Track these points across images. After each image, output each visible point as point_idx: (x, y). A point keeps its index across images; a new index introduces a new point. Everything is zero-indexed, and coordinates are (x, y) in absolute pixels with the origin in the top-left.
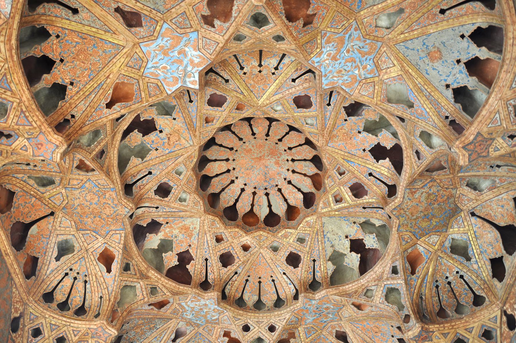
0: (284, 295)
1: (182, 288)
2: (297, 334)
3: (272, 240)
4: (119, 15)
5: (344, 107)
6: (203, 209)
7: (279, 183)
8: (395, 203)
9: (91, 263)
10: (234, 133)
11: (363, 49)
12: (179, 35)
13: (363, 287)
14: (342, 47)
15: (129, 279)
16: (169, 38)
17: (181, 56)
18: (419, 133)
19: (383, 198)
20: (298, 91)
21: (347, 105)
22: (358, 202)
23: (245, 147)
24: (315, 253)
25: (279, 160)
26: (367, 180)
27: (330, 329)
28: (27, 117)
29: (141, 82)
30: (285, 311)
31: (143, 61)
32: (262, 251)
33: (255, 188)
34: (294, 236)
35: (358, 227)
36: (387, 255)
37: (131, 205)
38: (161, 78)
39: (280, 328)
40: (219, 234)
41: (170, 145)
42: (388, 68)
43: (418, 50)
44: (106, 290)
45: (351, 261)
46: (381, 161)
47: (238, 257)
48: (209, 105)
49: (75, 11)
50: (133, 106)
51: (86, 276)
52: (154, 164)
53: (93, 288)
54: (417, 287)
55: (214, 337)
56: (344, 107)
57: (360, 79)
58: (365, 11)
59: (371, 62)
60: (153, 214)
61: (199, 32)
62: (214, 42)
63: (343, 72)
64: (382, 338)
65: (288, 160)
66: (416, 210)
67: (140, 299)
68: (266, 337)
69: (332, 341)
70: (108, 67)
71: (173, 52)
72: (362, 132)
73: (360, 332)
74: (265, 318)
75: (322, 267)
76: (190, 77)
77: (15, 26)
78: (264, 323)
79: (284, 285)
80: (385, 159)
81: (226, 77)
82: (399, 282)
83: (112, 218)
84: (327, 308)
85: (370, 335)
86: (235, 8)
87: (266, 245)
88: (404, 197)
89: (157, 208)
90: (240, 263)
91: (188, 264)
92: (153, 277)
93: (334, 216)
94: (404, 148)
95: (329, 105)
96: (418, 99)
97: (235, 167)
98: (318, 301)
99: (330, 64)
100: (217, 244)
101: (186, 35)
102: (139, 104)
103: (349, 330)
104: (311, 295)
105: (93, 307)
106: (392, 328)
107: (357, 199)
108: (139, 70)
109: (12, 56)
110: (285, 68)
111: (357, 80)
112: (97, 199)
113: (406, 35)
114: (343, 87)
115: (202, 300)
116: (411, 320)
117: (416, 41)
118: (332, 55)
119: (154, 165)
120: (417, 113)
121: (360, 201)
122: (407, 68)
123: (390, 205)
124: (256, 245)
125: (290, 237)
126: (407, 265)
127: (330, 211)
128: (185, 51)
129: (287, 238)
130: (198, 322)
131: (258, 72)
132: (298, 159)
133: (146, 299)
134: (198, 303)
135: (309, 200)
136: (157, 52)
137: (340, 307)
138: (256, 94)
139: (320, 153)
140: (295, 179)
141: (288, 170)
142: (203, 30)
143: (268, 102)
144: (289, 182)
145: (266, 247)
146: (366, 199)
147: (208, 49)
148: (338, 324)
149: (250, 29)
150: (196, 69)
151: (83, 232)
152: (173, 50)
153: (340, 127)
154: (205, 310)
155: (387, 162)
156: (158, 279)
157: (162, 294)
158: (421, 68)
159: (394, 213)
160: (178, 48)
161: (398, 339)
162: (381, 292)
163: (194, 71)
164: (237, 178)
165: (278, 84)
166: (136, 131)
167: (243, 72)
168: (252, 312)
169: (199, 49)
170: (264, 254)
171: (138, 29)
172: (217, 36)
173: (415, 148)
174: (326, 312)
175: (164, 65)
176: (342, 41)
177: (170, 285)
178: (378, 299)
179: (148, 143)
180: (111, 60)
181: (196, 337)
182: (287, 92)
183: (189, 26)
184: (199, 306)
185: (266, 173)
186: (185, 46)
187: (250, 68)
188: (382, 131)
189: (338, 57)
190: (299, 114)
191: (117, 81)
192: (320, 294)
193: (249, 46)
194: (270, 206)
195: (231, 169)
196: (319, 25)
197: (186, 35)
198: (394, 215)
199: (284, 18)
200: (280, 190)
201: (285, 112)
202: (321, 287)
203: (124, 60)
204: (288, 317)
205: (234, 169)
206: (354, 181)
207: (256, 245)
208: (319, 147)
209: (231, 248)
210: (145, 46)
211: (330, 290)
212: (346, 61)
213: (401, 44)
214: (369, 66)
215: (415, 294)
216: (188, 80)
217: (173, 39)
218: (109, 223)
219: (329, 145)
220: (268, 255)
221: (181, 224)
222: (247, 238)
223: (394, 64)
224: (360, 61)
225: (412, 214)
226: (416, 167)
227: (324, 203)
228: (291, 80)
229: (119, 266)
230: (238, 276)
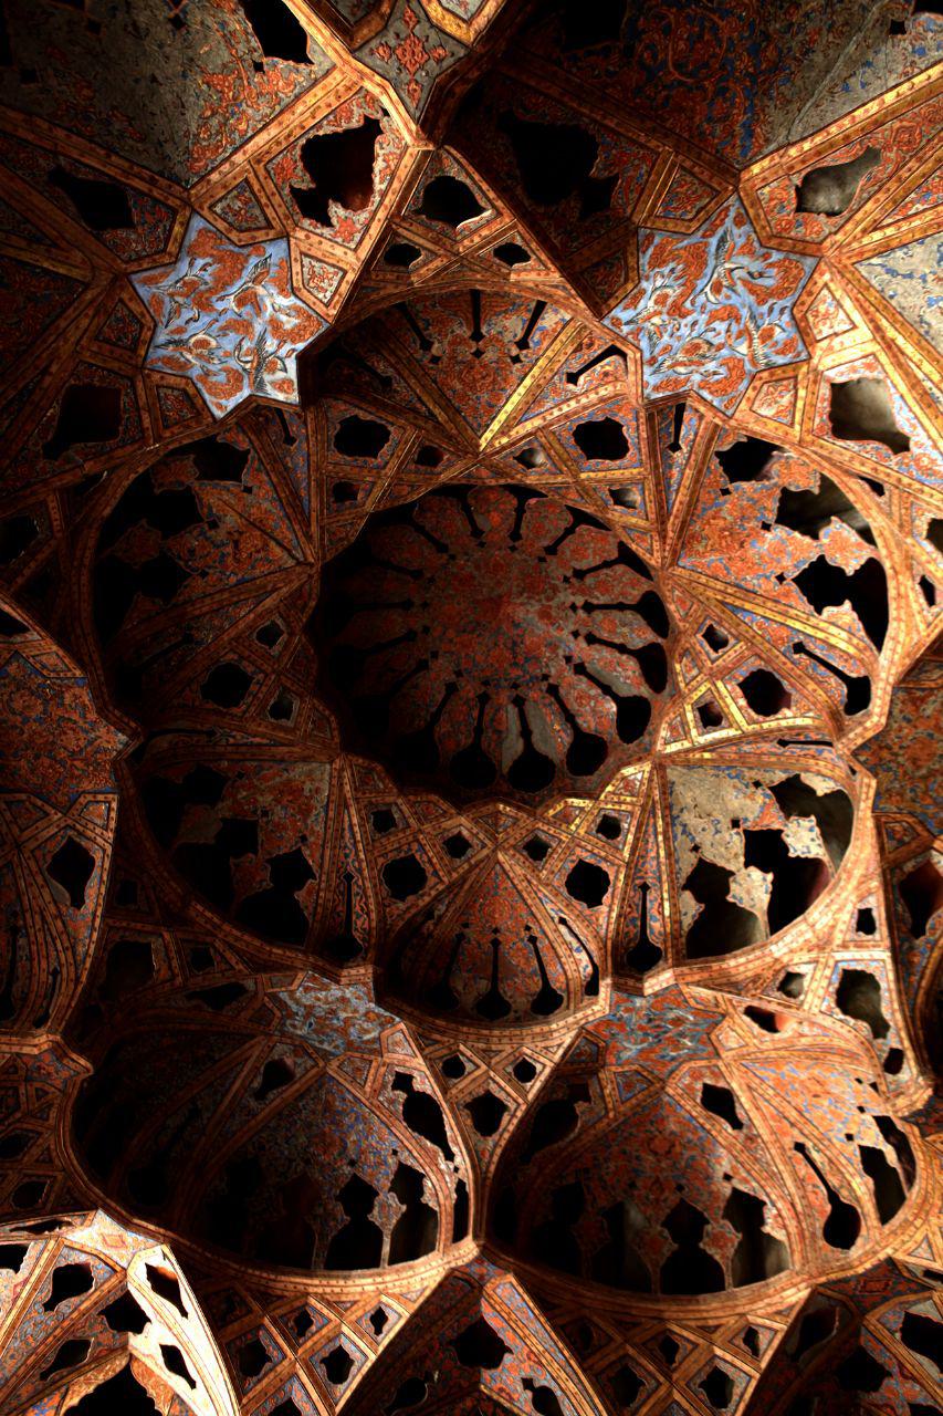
0: (562, 979)
1: (280, 952)
2: (593, 1090)
3: (529, 827)
6: (337, 740)
7: (553, 671)
8: (866, 729)
9: (31, 880)
10: (420, 529)
11: (759, 281)
12: (236, 249)
13: (778, 967)
14: (697, 278)
15: (133, 925)
16: (209, 260)
17: (247, 310)
18: (926, 527)
19: (834, 716)
20: (585, 408)
22: (765, 726)
23: (455, 570)
24: (648, 866)
25: (550, 607)
26: (789, 665)
27: (687, 1080)
29: (140, 386)
30: (562, 1023)
31: (142, 326)
32: (500, 856)
33: (486, 683)
34: (591, 818)
35: (766, 796)
36: (844, 876)
37: (133, 725)
38: (195, 373)
39: (547, 1071)
40: (384, 808)
41: (238, 561)
42: (836, 334)
43: (924, 279)
44: (70, 953)
45: (748, 892)
46: (828, 611)
47: (435, 873)
50: (120, 452)
51: (15, 914)
52: (197, 612)
53: (34, 948)
54: (928, 972)
55: (368, 1089)
56: (718, 454)
57: (754, 370)
58: (766, 163)
59: (786, 317)
60: (199, 750)
61: (293, 241)
62: (332, 270)
63: (705, 347)
64: (832, 1112)
65: (574, 607)
66: (927, 752)
67: (161, 977)
68: (509, 1095)
69: (694, 1114)
70: (44, 341)
71: (222, 299)
72: (774, 526)
73: (771, 1092)
74: (505, 1040)
75: (667, 905)
76: (273, 371)
78: (504, 1054)
79: (561, 954)
80: (839, 603)
81: (381, 367)
82: (875, 957)
83: (82, 760)
84: (678, 1021)
85: (799, 1101)
86: (379, 165)
87: (512, 841)
88: (890, 713)
89: (211, 734)
90: (441, 887)
91: (300, 889)
92: (202, 921)
93: (701, 763)
94: (889, 572)
95: (676, 447)
96: (922, 425)
97: (426, 622)
98: (652, 1001)
99: (664, 326)
100: (378, 835)
101: (257, 250)
102: (136, 446)
103: (740, 1085)
104: (631, 982)
105: (32, 997)
106: (860, 1087)
107: (761, 718)
108: (134, 351)
111: (743, 373)
112: (41, 708)
113: (890, 231)
114: (705, 394)
115: (334, 986)
116: (905, 1066)
117: (918, 250)
118: (670, 301)
119: (199, 617)
120: (919, 468)
121: (770, 723)
122: (891, 333)
123: (851, 735)
124: (487, 841)
125: (577, 821)
126: (900, 908)
127: (687, 751)
128: (256, 295)
129: (573, 822)
130: (326, 1046)
131: (470, 357)
132: (602, 602)
133: (179, 980)
134: (322, 995)
135: (635, 719)
136: (180, 299)
137: (713, 1018)
138: (470, 419)
139: (658, 583)
140: (598, 657)
141: (576, 634)
142: (301, 234)
143: (505, 440)
144: (580, 669)
145: (514, 847)
146: (787, 718)
148: (708, 1067)
149: (429, 229)
150: (288, 347)
151: (9, 797)
152: (223, 294)
153: (711, 513)
154: (343, 1015)
155: (845, 612)
156: (215, 926)
157: (224, 966)
158: (932, 332)
159: (862, 758)
160: (235, 289)
161: (875, 1117)
162: (825, 983)
163: (283, 352)
164: (435, 655)
165: (529, 390)
167: (428, 357)
168: (469, 1025)
169: (294, 291)
170: (507, 867)
171: (122, 233)
172: (339, 251)
173: (918, 571)
174: (673, 1030)
175: (201, 336)
176: (697, 259)
177: (248, 944)
178: (817, 1001)
179: (180, 558)
180: (53, 322)
181: (321, 1087)
182: (556, 413)
183: (263, 223)
184: (327, 1002)
185: (515, 643)
186: (254, 281)
187: (452, 343)
188: (829, 522)
189: (688, 304)
190: (592, 475)
192: (660, 981)
193: (433, 277)
194: (526, 733)
195: (418, 627)
196: (629, 211)
197: (257, 250)
198: (862, 763)
199: (519, 191)
200: (553, 690)
201: (554, 470)
202: (661, 962)
203: (87, 321)
204: (568, 1041)
205: (426, 630)
206: (754, 664)
207: (487, 841)
208: (654, 568)
209: (415, 846)
210: (146, 281)
211: (685, 969)
212: (713, 317)
213: (875, 261)
214: (778, 330)
215: (922, 992)
216: (267, 377)
217: (220, 260)
218: (76, 772)
219: (681, 563)
220: (518, 869)
221: (278, 779)
222: (463, 820)
223: (852, 322)
224: (753, 317)
225: (914, 764)
226: (922, 627)
227: (672, 728)
228: (564, 377)
229: (103, 890)
230: (436, 925)
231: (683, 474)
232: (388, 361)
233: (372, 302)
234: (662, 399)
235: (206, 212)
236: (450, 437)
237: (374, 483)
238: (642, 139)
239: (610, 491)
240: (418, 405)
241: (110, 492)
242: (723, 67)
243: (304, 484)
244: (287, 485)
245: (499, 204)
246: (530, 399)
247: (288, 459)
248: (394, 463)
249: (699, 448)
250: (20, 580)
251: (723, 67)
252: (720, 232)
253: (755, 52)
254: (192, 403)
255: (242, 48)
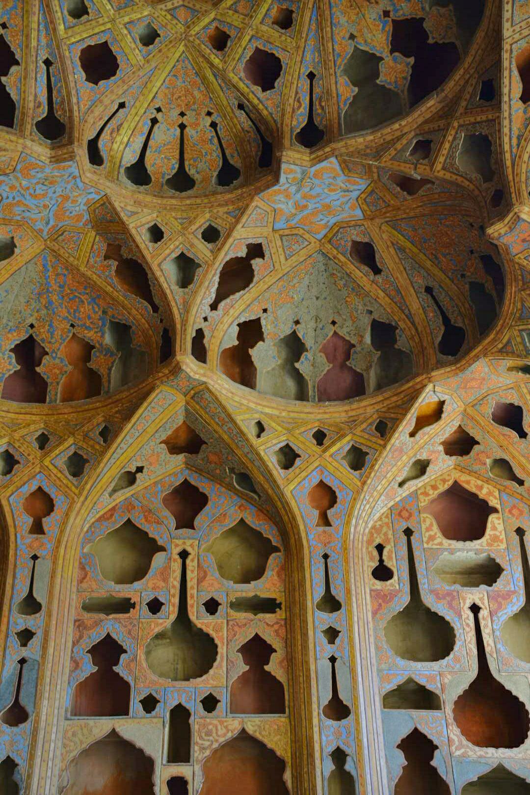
4: (378, 264)
5: (18, 63)
17: (304, 202)
20: (112, 92)
21: (14, 69)
28: (522, 276)
31: (365, 200)
48: (279, 60)
49: (429, 290)
56: (18, 63)
61: (271, 230)
77: (480, 348)
81: (242, 116)
95: (48, 63)
108: (373, 191)
109: (502, 326)
110: (140, 124)
114: (41, 164)
138: (190, 67)
142: (265, 234)
147: (260, 214)
150: (283, 188)
163: (288, 185)
166: (431, 41)
167: (214, 117)
171: (358, 239)
182: (131, 83)
183: (284, 238)
187: (199, 124)
189: (60, 200)
190: (102, 28)
191: (409, 197)
193: (197, 215)
199: (150, 276)
212: (44, 195)
216: (299, 176)
217: (311, 223)
224: (23, 196)
228: (127, 105)
231: (38, 41)
232: (239, 122)
233: (233, 203)
234: (65, 160)
235: (313, 240)
236: (203, 56)
237: (261, 23)
238: (94, 277)
239: (88, 13)
240: (223, 85)
241: (421, 120)
242: (63, 297)
243: (312, 34)
244: (323, 37)
245: (158, 274)
246: (149, 85)
247: (316, 60)
248: (244, 43)
249: (32, 67)
250: (490, 117)
251: (63, 297)
252: (50, 226)
253: (50, 303)
254: (346, 166)
255: (271, 318)
